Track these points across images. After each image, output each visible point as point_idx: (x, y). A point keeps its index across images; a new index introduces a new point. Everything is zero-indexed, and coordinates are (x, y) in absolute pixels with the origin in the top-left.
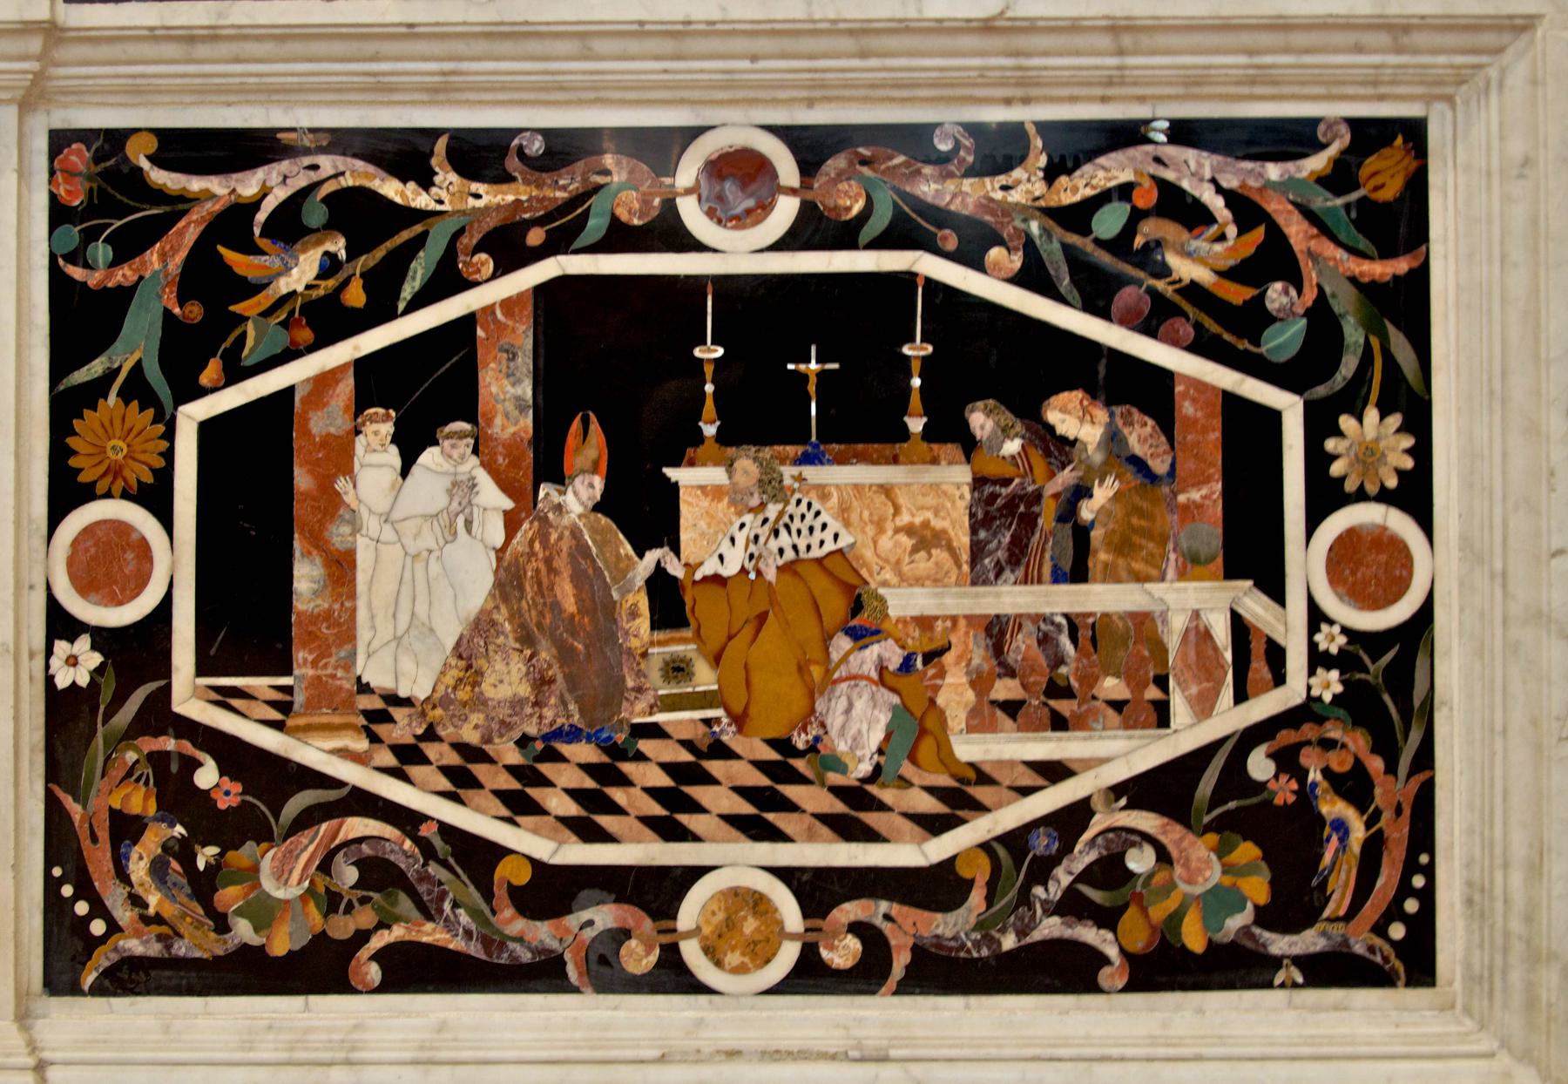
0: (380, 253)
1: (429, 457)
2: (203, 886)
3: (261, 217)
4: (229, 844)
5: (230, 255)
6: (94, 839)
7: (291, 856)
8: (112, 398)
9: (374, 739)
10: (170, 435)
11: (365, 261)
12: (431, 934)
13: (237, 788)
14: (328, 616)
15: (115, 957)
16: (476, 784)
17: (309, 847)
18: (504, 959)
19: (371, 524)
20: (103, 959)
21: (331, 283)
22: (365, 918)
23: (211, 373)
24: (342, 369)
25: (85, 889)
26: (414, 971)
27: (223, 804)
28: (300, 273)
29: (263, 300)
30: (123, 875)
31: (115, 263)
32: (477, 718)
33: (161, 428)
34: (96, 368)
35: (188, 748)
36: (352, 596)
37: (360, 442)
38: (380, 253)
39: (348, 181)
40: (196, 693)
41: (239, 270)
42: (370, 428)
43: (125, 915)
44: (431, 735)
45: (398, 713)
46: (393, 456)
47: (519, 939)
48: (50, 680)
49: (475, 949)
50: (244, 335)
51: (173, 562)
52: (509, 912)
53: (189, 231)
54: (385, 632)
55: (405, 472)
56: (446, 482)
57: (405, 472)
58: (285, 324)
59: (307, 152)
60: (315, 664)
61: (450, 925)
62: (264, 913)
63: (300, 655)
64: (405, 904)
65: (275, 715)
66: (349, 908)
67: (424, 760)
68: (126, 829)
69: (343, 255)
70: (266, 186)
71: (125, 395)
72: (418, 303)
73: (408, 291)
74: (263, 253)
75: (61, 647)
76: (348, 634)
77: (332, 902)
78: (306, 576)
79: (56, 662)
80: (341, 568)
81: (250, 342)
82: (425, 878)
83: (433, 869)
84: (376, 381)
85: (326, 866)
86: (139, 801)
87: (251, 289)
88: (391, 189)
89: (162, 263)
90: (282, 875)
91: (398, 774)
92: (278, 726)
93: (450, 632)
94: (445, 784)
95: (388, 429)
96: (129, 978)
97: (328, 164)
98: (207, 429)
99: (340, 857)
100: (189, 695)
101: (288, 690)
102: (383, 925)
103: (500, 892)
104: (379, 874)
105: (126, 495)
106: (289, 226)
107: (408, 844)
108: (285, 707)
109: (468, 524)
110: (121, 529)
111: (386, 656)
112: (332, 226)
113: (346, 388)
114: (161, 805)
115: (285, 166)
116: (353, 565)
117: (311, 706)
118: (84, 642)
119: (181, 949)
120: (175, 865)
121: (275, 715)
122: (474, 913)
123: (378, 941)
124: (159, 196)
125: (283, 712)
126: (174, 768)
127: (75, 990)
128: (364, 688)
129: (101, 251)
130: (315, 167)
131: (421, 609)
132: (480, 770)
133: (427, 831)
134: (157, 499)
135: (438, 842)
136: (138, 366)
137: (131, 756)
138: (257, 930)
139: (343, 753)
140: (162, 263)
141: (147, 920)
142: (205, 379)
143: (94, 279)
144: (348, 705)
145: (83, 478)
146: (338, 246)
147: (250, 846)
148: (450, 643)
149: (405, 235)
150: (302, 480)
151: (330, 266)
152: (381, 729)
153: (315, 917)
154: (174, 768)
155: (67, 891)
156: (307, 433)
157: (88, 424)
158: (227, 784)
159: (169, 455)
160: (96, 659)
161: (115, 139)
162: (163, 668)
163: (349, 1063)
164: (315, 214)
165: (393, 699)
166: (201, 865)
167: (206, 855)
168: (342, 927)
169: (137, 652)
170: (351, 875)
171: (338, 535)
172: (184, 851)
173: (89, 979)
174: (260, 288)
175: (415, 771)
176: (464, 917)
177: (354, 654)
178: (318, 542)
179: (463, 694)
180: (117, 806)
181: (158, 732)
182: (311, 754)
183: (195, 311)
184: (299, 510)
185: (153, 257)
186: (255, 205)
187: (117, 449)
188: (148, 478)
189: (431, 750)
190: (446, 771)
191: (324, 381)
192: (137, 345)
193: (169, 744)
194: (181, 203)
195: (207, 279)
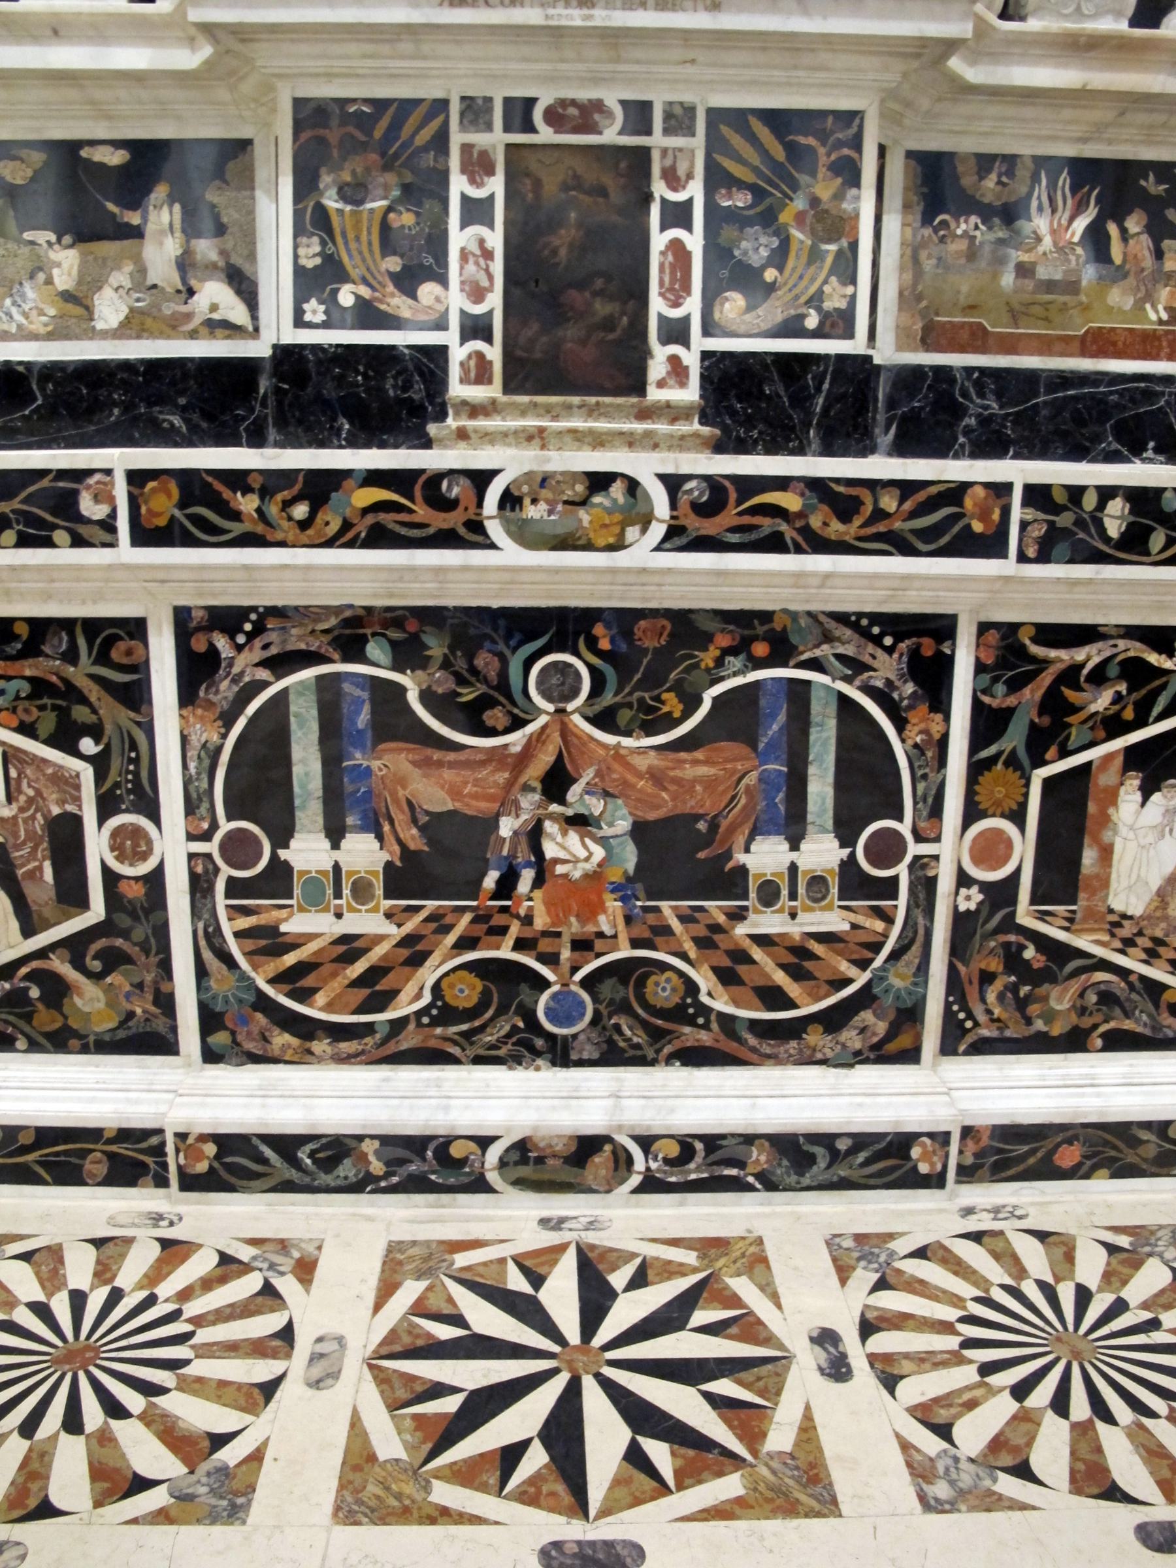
0: (1143, 692)
1: (1156, 797)
2: (1022, 1005)
3: (1085, 672)
4: (1036, 984)
5: (1068, 693)
6: (971, 982)
7: (1066, 990)
8: (1000, 766)
9: (1113, 935)
10: (1027, 785)
11: (1135, 696)
12: (1128, 1025)
13: (1044, 958)
14: (1097, 876)
15: (975, 1038)
16: (1158, 956)
17: (1075, 986)
18: (1160, 1036)
19: (1123, 830)
20: (970, 1038)
21: (1117, 707)
22: (1097, 1018)
23: (1051, 753)
24: (1117, 752)
25: (965, 1008)
26: (1118, 1042)
27: (1036, 966)
28: (1102, 702)
29: (1082, 715)
30: (983, 1000)
31: (1007, 695)
32: (1163, 925)
33: (1023, 781)
34: (992, 750)
35: (1022, 940)
36: (1110, 866)
37: (1122, 790)
38: (1143, 692)
39: (1131, 654)
40: (1028, 913)
41: (1071, 700)
42: (1128, 782)
43: (982, 1018)
44: (1140, 933)
45: (1126, 923)
46: (1138, 797)
47: (1169, 1027)
48: (956, 907)
49: (1147, 1032)
50: (1069, 735)
51: (1023, 850)
52: (1166, 1015)
53: (1046, 679)
54: (1124, 883)
55: (1143, 804)
56: (1162, 810)
57: (1143, 804)
58: (1092, 728)
59: (1112, 637)
60: (1088, 899)
61: (1137, 1021)
62: (1050, 1016)
63: (1082, 895)
64: (1117, 1011)
65: (1067, 924)
66: (1091, 1014)
67: (1135, 945)
68: (987, 978)
69: (1124, 692)
70: (1090, 655)
71: (1007, 764)
72: (1159, 718)
73: (1156, 711)
74: (1083, 690)
75: (963, 891)
76: (1105, 883)
77: (1083, 1011)
78: (1089, 857)
79: (960, 899)
80: (1106, 853)
81: (1072, 738)
82: (1128, 999)
83: (1134, 996)
84: (1135, 758)
85: (1081, 995)
86: (995, 965)
87: (1075, 709)
88: (1153, 658)
89: (1032, 694)
90: (1060, 1000)
91: (1122, 952)
92: (1067, 929)
93: (1155, 883)
94: (1144, 956)
95: (1137, 782)
96: (982, 1047)
97: (1122, 644)
98: (1048, 783)
99: (1088, 992)
100: (1025, 914)
101: (1073, 912)
102: (1106, 1021)
103: (1163, 1005)
104: (1107, 998)
105: (1003, 816)
106: (1099, 677)
107: (1123, 984)
108: (1071, 920)
109: (1171, 831)
110: (999, 832)
111: (1122, 896)
112: (1121, 677)
113: (1119, 761)
114: (1006, 967)
115: (1100, 645)
116: (1112, 852)
117: (1085, 919)
118: (974, 890)
119: (1008, 1033)
120: (1009, 995)
121: (1067, 924)
122: (1150, 1016)
123: (1102, 1029)
124: (1034, 659)
125: (1070, 923)
126: (1014, 949)
127: (954, 1052)
128: (1111, 911)
129: (1000, 688)
130: (1115, 646)
131: (1143, 874)
132: (1161, 950)
133: (1133, 978)
134: (1018, 817)
135: (1137, 984)
136: (1013, 752)
137: (993, 944)
138: (1045, 1024)
139: (1098, 942)
140: (1032, 694)
141: (993, 1021)
142: (1048, 756)
143: (995, 703)
144: (1102, 919)
145: (981, 807)
146: (1123, 688)
147: (1046, 986)
148: (1155, 888)
149: (1157, 683)
150: (1092, 808)
151: (1118, 698)
152: (1117, 931)
153: (1074, 1019)
154: (1014, 949)
155: (955, 1008)
156: (1097, 785)
157: (986, 778)
158: (1039, 956)
159: (1026, 795)
160: (981, 897)
161: (1014, 627)
162: (1013, 901)
163: (1092, 1086)
164: (1113, 671)
165: (1124, 916)
166: (1022, 994)
167: (1025, 990)
168: (1086, 1022)
169: (1002, 894)
170: (1094, 998)
171: (1106, 836)
172: (1014, 989)
173: (962, 1048)
174: (1081, 709)
175: (1131, 950)
176: (1144, 1017)
177: (1107, 895)
178: (1097, 841)
179: (1158, 914)
180: (983, 966)
181: (1007, 932)
182: (1082, 942)
183: (1046, 721)
184: (1089, 824)
185: (1026, 691)
186: (1082, 666)
187: (1000, 792)
188: (1015, 807)
189: (1140, 941)
190: (1146, 950)
191: (1108, 758)
192: (1014, 739)
193: (1012, 938)
194: (1045, 663)
195: (1056, 707)
